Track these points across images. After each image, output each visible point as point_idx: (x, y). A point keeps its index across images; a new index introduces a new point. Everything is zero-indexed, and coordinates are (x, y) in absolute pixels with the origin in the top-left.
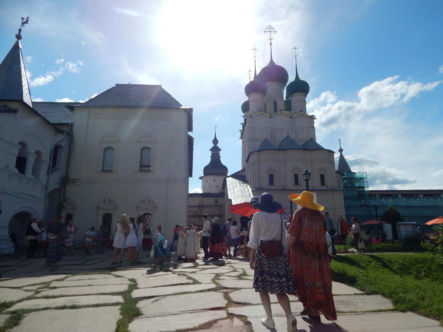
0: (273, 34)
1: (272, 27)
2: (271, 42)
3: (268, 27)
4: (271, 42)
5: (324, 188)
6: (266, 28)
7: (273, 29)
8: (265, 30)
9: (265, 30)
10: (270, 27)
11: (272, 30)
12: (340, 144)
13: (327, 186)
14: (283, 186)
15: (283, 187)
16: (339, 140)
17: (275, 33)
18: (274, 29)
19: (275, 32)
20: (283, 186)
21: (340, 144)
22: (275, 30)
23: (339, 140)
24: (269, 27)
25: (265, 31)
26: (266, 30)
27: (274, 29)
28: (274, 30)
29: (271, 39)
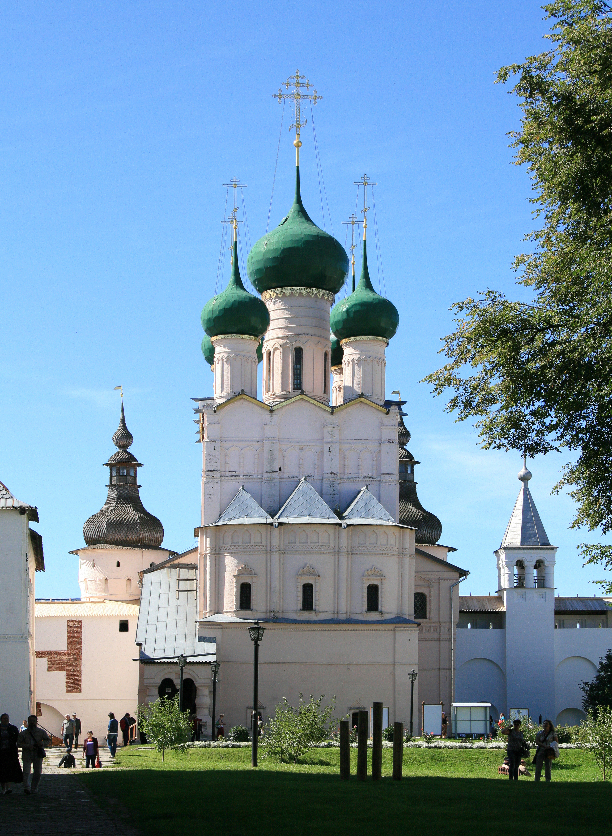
1: (303, 77)
3: (292, 77)
6: (283, 84)
7: (308, 85)
8: (280, 90)
9: (280, 90)
11: (302, 90)
13: (382, 613)
14: (273, 612)
15: (273, 614)
18: (312, 86)
20: (273, 612)
22: (315, 91)
26: (285, 90)
27: (312, 86)
28: (311, 92)
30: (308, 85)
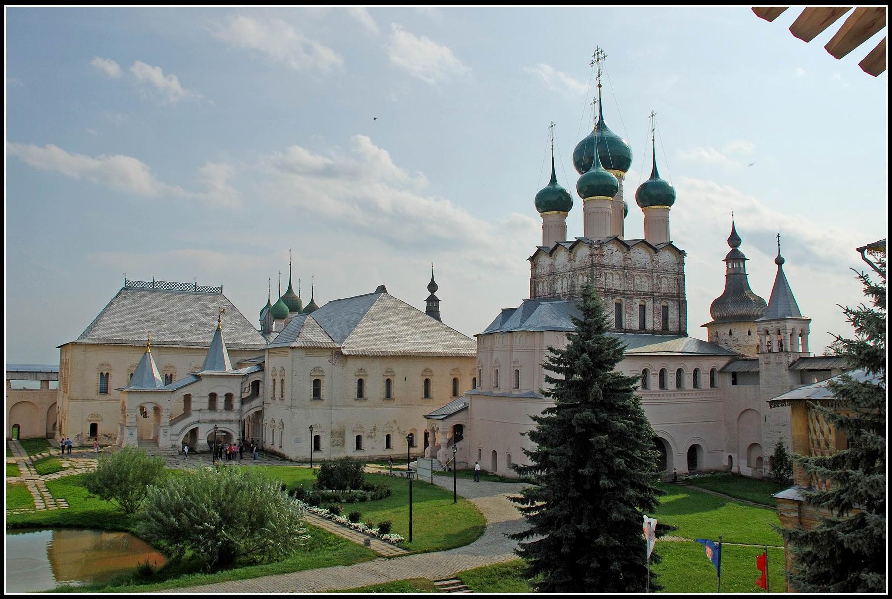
0: (601, 61)
1: (600, 48)
2: (599, 81)
3: (595, 51)
4: (599, 81)
5: (516, 393)
10: (597, 50)
12: (779, 245)
16: (778, 234)
17: (605, 60)
19: (604, 57)
21: (779, 245)
23: (778, 234)
24: (596, 52)
25: (592, 63)
29: (599, 76)
30: (601, 52)
